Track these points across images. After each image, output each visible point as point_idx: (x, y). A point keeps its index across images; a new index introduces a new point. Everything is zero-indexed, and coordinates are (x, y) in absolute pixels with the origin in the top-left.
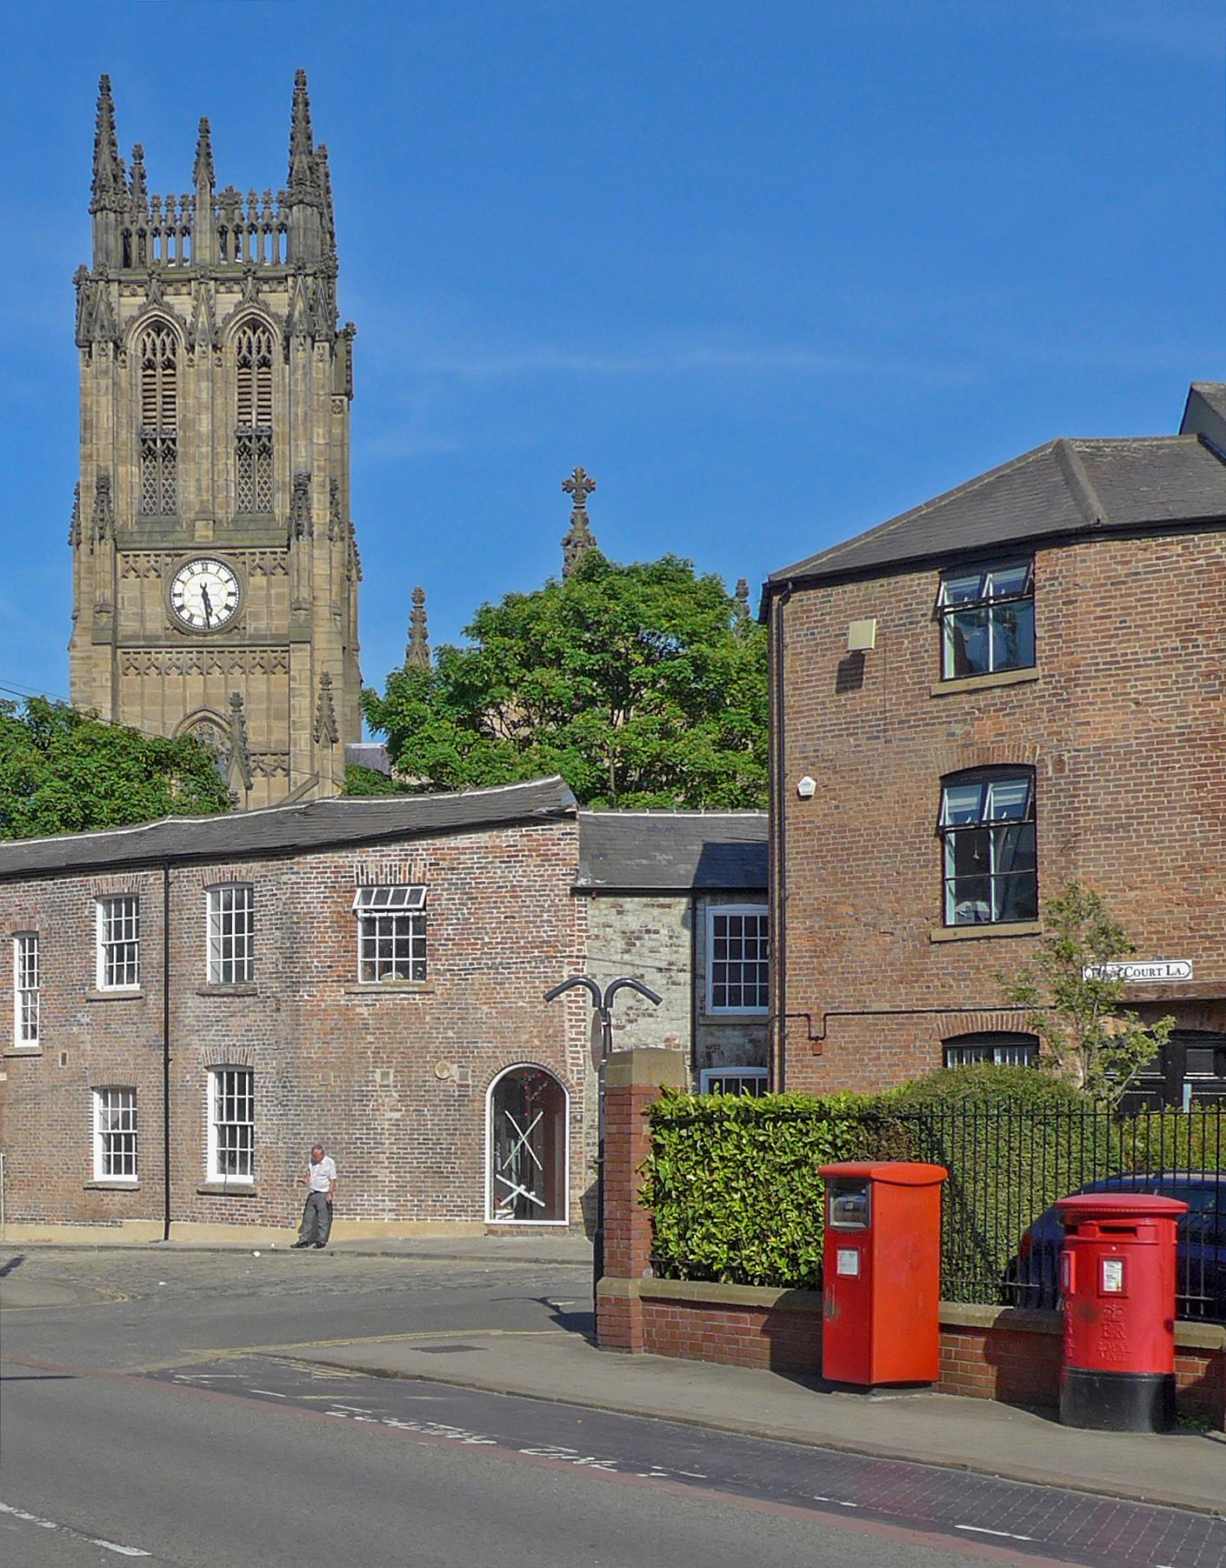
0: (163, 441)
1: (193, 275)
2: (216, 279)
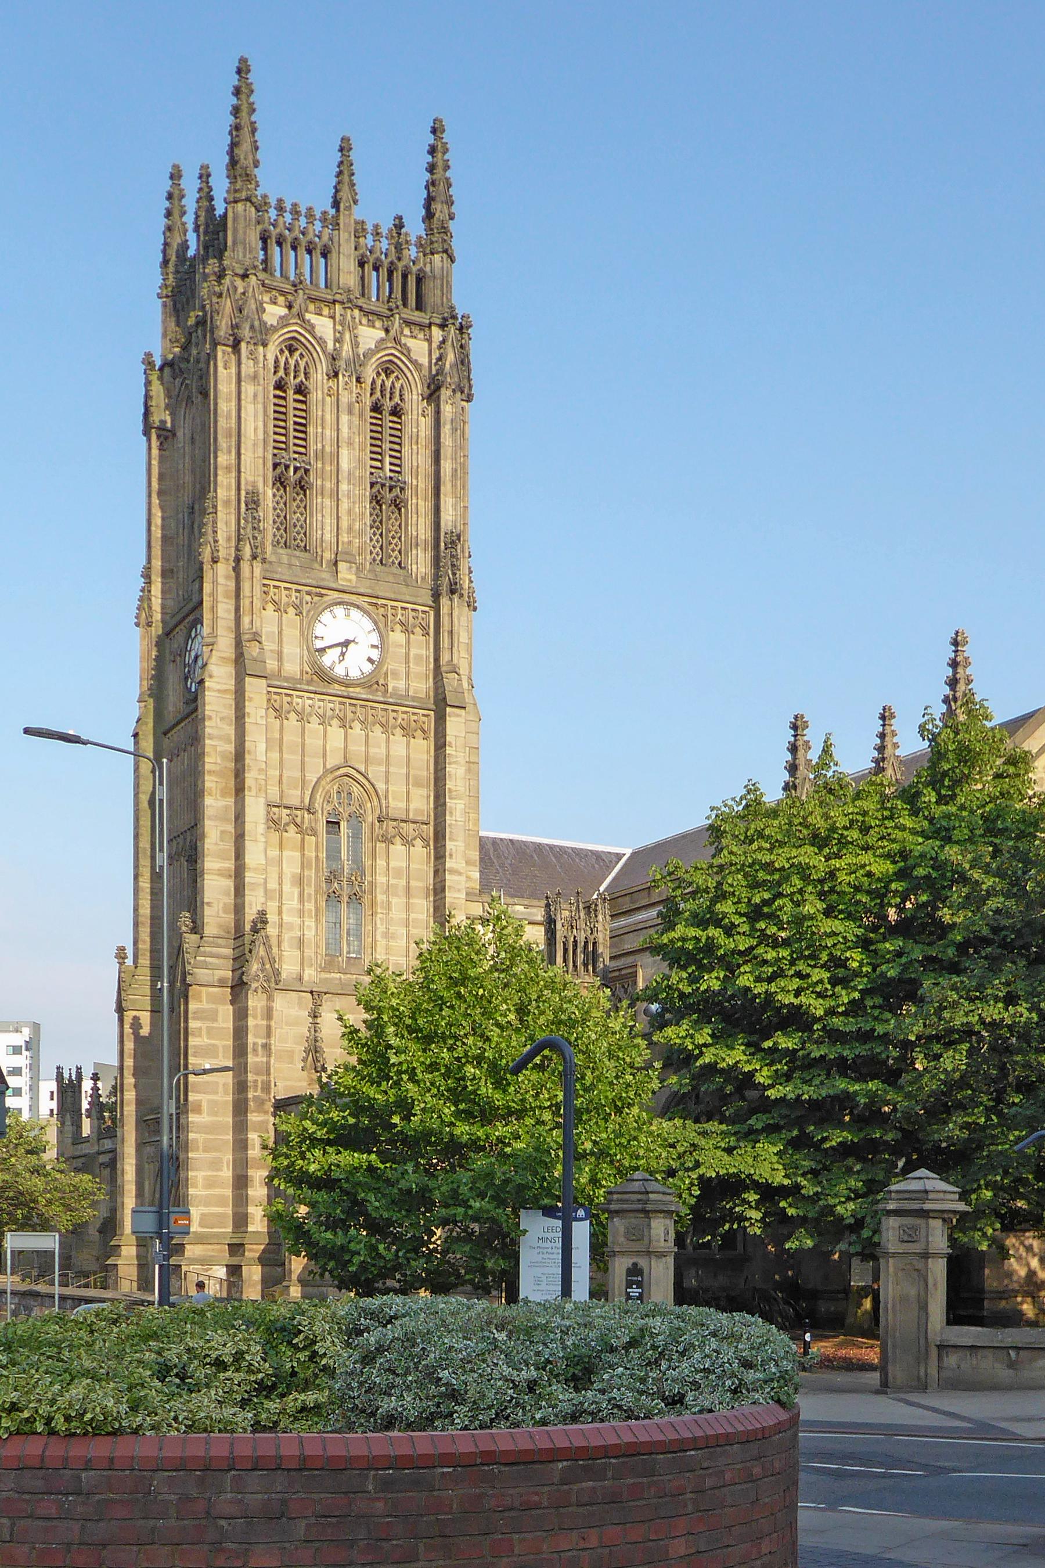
0: (296, 469)
1: (338, 297)
2: (361, 309)
